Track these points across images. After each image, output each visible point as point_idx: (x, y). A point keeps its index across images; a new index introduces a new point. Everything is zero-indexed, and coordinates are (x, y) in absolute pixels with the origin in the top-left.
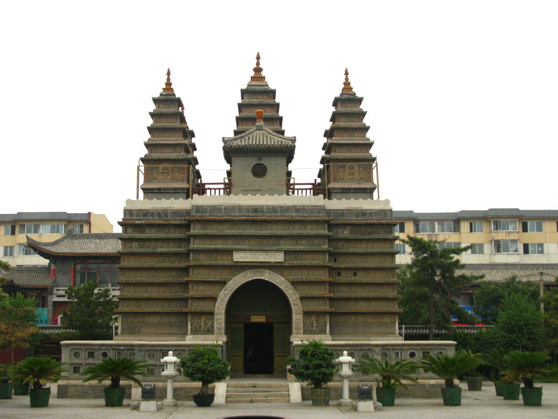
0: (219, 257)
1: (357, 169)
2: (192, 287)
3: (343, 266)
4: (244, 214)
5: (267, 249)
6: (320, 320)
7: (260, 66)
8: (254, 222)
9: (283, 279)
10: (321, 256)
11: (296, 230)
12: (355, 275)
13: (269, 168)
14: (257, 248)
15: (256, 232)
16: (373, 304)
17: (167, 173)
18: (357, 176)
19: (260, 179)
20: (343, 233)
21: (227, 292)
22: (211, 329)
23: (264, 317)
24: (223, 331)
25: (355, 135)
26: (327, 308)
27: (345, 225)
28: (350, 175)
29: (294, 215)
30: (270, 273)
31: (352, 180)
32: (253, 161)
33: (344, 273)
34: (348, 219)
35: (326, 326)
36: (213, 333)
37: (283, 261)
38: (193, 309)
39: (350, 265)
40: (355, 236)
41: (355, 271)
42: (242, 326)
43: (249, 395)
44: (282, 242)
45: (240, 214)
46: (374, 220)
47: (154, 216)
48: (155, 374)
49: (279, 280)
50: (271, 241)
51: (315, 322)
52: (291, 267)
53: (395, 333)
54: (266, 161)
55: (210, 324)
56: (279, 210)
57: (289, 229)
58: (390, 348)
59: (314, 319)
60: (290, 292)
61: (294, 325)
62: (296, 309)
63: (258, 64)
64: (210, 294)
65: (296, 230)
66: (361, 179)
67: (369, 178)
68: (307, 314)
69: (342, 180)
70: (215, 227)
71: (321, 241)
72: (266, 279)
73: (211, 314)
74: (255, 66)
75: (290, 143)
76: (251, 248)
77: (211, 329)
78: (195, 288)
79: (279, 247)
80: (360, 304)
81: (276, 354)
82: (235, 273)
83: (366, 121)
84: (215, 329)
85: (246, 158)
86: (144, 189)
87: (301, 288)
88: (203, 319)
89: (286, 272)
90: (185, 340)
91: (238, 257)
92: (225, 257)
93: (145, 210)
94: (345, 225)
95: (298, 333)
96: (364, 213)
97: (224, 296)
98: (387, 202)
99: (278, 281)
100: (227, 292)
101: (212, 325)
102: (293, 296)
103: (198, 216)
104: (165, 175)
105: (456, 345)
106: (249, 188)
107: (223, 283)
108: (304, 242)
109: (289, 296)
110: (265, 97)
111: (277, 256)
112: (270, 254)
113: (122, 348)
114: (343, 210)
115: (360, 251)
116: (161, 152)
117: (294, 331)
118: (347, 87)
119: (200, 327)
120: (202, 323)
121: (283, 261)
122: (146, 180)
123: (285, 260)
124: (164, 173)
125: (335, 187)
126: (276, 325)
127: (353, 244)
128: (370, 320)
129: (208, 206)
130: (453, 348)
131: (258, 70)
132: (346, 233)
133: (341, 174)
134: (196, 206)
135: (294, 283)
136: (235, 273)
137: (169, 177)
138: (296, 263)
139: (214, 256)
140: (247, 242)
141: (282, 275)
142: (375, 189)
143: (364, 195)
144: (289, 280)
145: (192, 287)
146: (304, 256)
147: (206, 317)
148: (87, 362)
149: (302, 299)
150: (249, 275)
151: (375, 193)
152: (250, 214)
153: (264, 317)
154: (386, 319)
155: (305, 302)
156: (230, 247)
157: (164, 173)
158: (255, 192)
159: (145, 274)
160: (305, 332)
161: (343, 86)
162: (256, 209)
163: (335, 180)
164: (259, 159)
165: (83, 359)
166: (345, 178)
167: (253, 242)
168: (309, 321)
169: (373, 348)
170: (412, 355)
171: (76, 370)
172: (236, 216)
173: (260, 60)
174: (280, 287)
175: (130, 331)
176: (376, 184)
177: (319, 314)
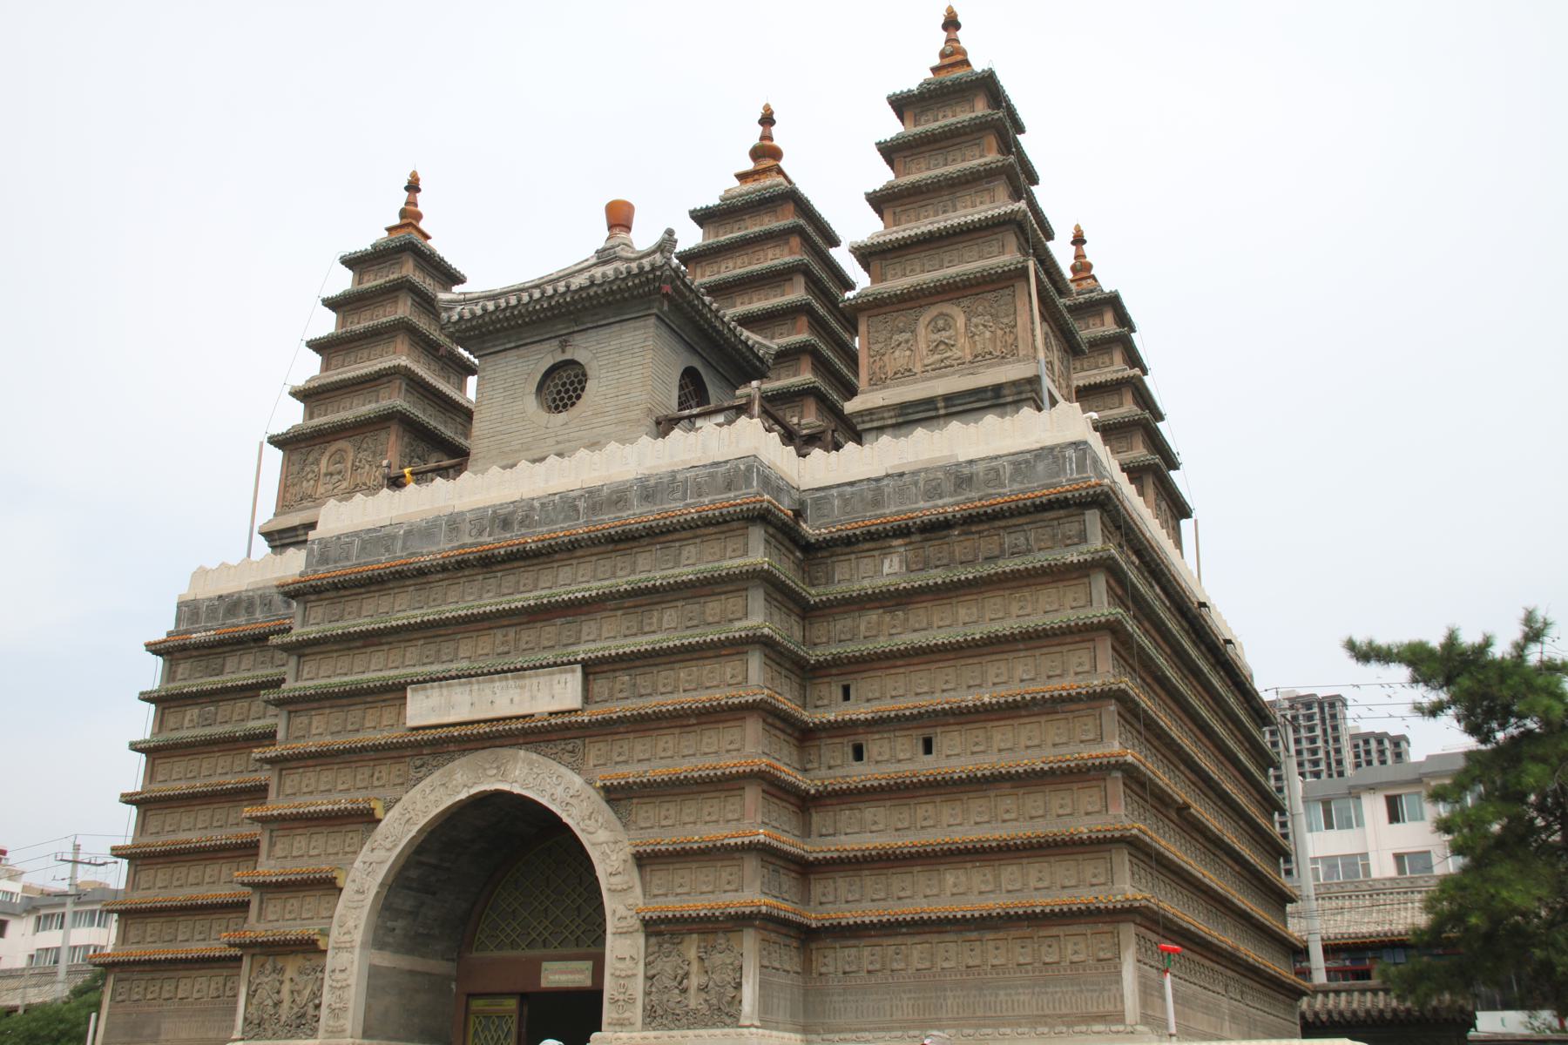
1: (961, 321)
2: (272, 845)
4: (468, 540)
5: (519, 661)
6: (718, 958)
7: (777, 142)
9: (577, 781)
16: (1011, 874)
17: (339, 473)
18: (962, 349)
20: (878, 572)
21: (380, 854)
22: (311, 1011)
25: (959, 205)
27: (878, 538)
29: (637, 515)
30: (531, 763)
31: (941, 368)
32: (544, 357)
34: (892, 512)
39: (907, 704)
41: (925, 726)
42: (511, 1004)
46: (1010, 492)
49: (556, 786)
50: (548, 632)
51: (695, 967)
52: (607, 728)
53: (1119, 1018)
55: (307, 992)
56: (581, 505)
59: (692, 954)
60: (602, 835)
62: (622, 911)
63: (766, 137)
68: (658, 929)
69: (907, 374)
72: (517, 790)
73: (309, 948)
77: (311, 1011)
78: (279, 850)
84: (324, 1012)
85: (522, 351)
86: (268, 535)
88: (290, 972)
89: (594, 752)
91: (426, 709)
93: (230, 595)
94: (878, 538)
95: (621, 1024)
97: (367, 869)
99: (559, 791)
100: (380, 854)
101: (317, 994)
107: (366, 819)
111: (557, 689)
112: (533, 682)
114: (877, 480)
115: (941, 637)
120: (286, 988)
122: (284, 505)
123: (587, 697)
124: (331, 474)
125: (869, 405)
128: (994, 952)
129: (356, 534)
132: (891, 570)
135: (616, 795)
137: (345, 484)
140: (466, 648)
141: (577, 770)
145: (272, 845)
149: (645, 861)
150: (459, 777)
154: (1075, 947)
155: (660, 878)
156: (392, 674)
157: (331, 474)
159: (203, 815)
162: (503, 519)
163: (878, 382)
166: (918, 369)
168: (667, 966)
173: (774, 130)
174: (565, 819)
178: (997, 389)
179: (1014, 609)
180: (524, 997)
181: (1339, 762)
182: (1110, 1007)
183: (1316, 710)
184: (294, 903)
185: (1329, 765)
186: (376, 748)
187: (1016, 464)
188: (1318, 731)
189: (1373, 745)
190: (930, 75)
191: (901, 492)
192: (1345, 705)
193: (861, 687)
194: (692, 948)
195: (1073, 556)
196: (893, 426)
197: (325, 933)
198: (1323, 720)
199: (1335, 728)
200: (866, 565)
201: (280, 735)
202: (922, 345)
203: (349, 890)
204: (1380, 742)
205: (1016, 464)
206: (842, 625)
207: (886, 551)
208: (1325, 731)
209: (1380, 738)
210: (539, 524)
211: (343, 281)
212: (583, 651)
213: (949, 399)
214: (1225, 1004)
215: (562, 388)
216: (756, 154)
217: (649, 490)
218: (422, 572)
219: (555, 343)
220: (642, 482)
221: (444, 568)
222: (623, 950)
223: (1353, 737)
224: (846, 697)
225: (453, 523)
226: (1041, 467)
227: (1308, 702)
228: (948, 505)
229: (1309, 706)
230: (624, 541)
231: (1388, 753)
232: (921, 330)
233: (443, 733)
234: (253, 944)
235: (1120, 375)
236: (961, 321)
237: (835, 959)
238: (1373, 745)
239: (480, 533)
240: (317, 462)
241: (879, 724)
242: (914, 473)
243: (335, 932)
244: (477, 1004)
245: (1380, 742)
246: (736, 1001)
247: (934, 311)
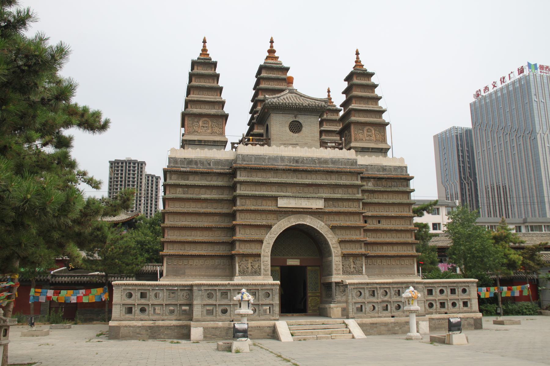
0: (264, 203)
1: (373, 132)
3: (369, 214)
6: (358, 262)
7: (274, 48)
8: (296, 171)
9: (323, 224)
10: (356, 204)
11: (333, 180)
12: (379, 223)
13: (303, 124)
14: (300, 195)
15: (297, 180)
18: (373, 138)
19: (297, 135)
20: (367, 185)
23: (299, 260)
24: (270, 273)
26: (363, 251)
29: (331, 167)
30: (312, 219)
31: (370, 141)
32: (290, 118)
33: (369, 221)
35: (362, 267)
36: (260, 274)
38: (241, 252)
39: (375, 213)
40: (376, 189)
41: (379, 219)
43: (312, 332)
44: (321, 190)
45: (283, 164)
46: (393, 174)
47: (197, 165)
48: (434, 294)
50: (311, 189)
51: (352, 263)
54: (301, 119)
55: (257, 266)
56: (317, 161)
57: (326, 179)
59: (352, 261)
60: (330, 236)
61: (334, 267)
63: (271, 47)
64: (256, 237)
65: (333, 180)
66: (377, 141)
67: (384, 140)
68: (345, 256)
70: (259, 174)
71: (355, 191)
72: (308, 224)
73: (259, 255)
74: (269, 48)
75: (323, 103)
76: (294, 195)
79: (319, 195)
80: (384, 248)
81: (309, 294)
82: (279, 218)
83: (378, 92)
84: (262, 271)
85: (284, 115)
87: (338, 232)
88: (250, 261)
89: (325, 218)
90: (233, 280)
91: (282, 203)
92: (269, 203)
93: (189, 159)
95: (338, 274)
96: (384, 169)
97: (270, 239)
98: (402, 160)
99: (319, 225)
101: (259, 266)
102: (332, 239)
103: (244, 164)
104: (206, 128)
105: (477, 283)
106: (287, 142)
107: (269, 227)
108: (340, 190)
109: (329, 240)
110: (280, 73)
111: (318, 203)
112: (311, 201)
113: (176, 288)
116: (200, 108)
117: (334, 272)
118: (358, 64)
126: (309, 268)
127: (376, 195)
128: (393, 262)
129: (253, 155)
130: (475, 285)
131: (271, 51)
134: (242, 155)
135: (333, 228)
136: (279, 218)
137: (209, 131)
138: (335, 209)
139: (259, 202)
140: (289, 189)
142: (389, 149)
143: (380, 154)
144: (329, 226)
146: (340, 203)
147: (253, 258)
148: (139, 302)
149: (341, 242)
151: (389, 153)
152: (291, 164)
153: (299, 260)
154: (407, 261)
155: (343, 245)
158: (295, 145)
159: (189, 218)
160: (345, 272)
161: (355, 64)
162: (296, 160)
163: (356, 140)
165: (136, 300)
167: (294, 189)
168: (347, 263)
170: (442, 292)
171: (129, 311)
172: (280, 165)
175: (176, 273)
176: (390, 145)
177: (356, 256)
179: (394, 197)
181: (141, 183)
183: (136, 165)
185: (138, 183)
187: (394, 168)
188: (136, 172)
189: (150, 178)
191: (372, 169)
192: (145, 165)
194: (351, 260)
196: (360, 151)
198: (138, 168)
199: (141, 172)
203: (265, 243)
204: (152, 178)
205: (394, 168)
207: (369, 181)
208: (138, 172)
209: (153, 177)
210: (306, 163)
212: (325, 195)
213: (372, 148)
215: (296, 127)
216: (269, 51)
217: (334, 161)
219: (293, 115)
220: (332, 159)
223: (146, 175)
225: (282, 158)
226: (399, 170)
227: (135, 162)
228: (381, 174)
229: (134, 164)
231: (154, 181)
232: (365, 131)
233: (289, 209)
236: (373, 132)
238: (150, 178)
239: (290, 163)
241: (372, 217)
242: (375, 166)
245: (152, 178)
247: (368, 127)
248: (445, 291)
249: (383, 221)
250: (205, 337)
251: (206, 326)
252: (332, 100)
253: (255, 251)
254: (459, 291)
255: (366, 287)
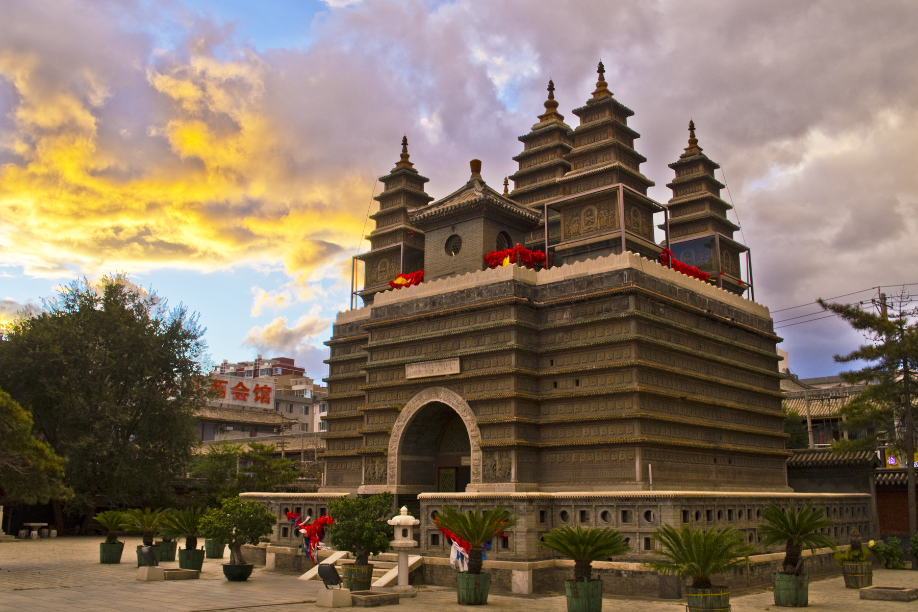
1: (596, 213)
2: (368, 419)
6: (504, 460)
9: (460, 398)
11: (481, 323)
12: (577, 385)
13: (463, 238)
16: (602, 430)
18: (597, 224)
21: (401, 423)
28: (587, 224)
29: (475, 302)
32: (446, 234)
35: (510, 469)
36: (385, 483)
37: (458, 371)
40: (580, 320)
41: (576, 376)
42: (453, 471)
53: (634, 479)
54: (461, 231)
58: (571, 503)
59: (497, 458)
60: (468, 417)
63: (551, 96)
68: (487, 450)
69: (577, 234)
72: (442, 401)
84: (388, 476)
91: (413, 372)
94: (563, 305)
95: (476, 481)
97: (399, 427)
100: (401, 423)
101: (386, 470)
107: (396, 411)
108: (487, 340)
115: (580, 344)
117: (472, 478)
119: (374, 473)
120: (376, 468)
121: (458, 371)
123: (462, 369)
128: (598, 456)
132: (564, 318)
133: (575, 226)
145: (368, 419)
149: (481, 426)
150: (424, 397)
154: (621, 455)
155: (487, 432)
160: (486, 479)
163: (568, 237)
164: (453, 229)
166: (582, 232)
167: (430, 348)
168: (489, 462)
169: (515, 504)
178: (608, 241)
180: (457, 469)
182: (631, 476)
184: (376, 440)
186: (397, 386)
190: (592, 97)
193: (559, 361)
195: (623, 315)
197: (386, 450)
200: (558, 315)
201: (367, 380)
202: (583, 222)
203: (393, 435)
206: (550, 338)
211: (381, 188)
212: (460, 352)
213: (591, 245)
214: (713, 467)
217: (479, 290)
218: (408, 322)
221: (415, 321)
222: (475, 459)
224: (552, 364)
230: (473, 312)
232: (582, 216)
233: (417, 381)
234: (365, 454)
235: (705, 195)
236: (596, 213)
237: (548, 458)
240: (377, 267)
241: (562, 375)
243: (389, 449)
244: (442, 471)
246: (510, 474)
248: (613, 516)
249: (584, 382)
250: (276, 566)
251: (280, 552)
252: (699, 144)
253: (377, 449)
254: (636, 515)
255: (443, 504)
